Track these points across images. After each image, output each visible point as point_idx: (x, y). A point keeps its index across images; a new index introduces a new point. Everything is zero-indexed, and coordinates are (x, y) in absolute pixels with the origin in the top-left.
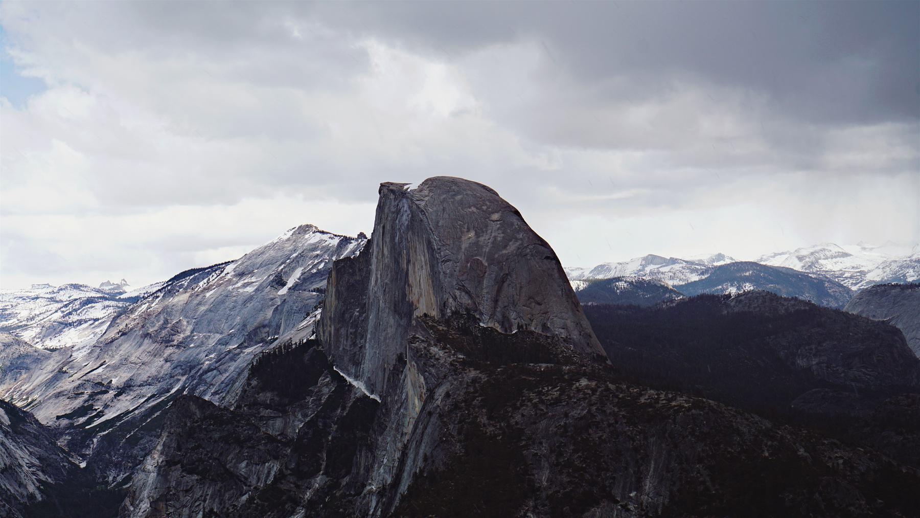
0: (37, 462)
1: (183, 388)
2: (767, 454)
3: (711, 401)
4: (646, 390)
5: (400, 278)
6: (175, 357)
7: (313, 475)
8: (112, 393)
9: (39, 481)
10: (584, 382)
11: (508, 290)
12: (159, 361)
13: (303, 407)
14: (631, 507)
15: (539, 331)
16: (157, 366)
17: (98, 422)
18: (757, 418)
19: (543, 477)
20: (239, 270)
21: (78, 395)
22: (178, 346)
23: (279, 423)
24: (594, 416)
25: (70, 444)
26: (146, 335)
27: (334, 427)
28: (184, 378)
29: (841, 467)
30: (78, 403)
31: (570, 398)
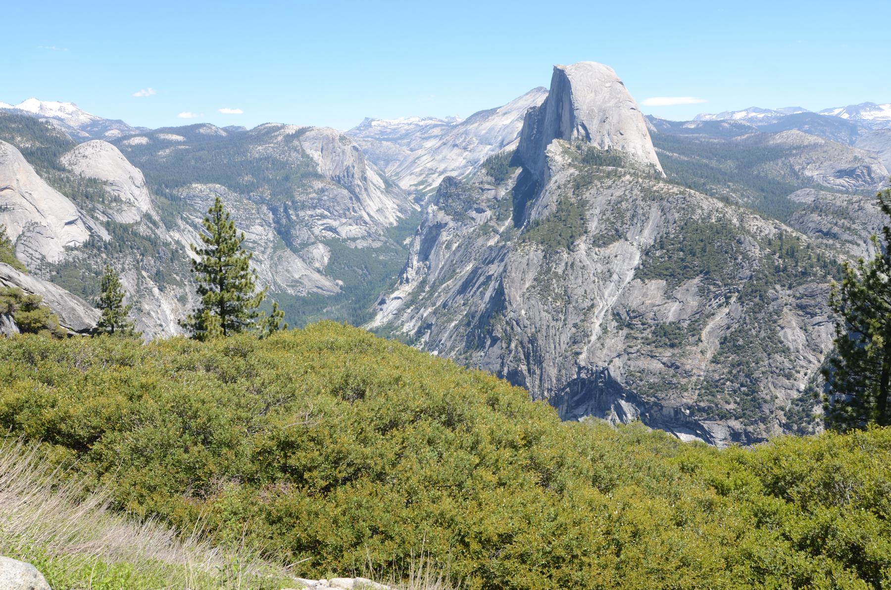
0: (396, 207)
1: (470, 173)
2: (714, 221)
3: (692, 191)
4: (658, 183)
5: (559, 117)
6: (468, 157)
7: (507, 219)
8: (437, 175)
9: (397, 216)
10: (628, 177)
11: (607, 126)
12: (461, 159)
13: (507, 185)
14: (635, 244)
15: (620, 149)
16: (461, 162)
17: (429, 188)
18: (715, 201)
19: (593, 226)
20: (504, 111)
21: (421, 175)
22: (470, 151)
23: (493, 192)
24: (626, 196)
25: (415, 199)
26: (455, 145)
27: (520, 196)
28: (471, 168)
29: (755, 230)
30: (421, 178)
31: (617, 185)
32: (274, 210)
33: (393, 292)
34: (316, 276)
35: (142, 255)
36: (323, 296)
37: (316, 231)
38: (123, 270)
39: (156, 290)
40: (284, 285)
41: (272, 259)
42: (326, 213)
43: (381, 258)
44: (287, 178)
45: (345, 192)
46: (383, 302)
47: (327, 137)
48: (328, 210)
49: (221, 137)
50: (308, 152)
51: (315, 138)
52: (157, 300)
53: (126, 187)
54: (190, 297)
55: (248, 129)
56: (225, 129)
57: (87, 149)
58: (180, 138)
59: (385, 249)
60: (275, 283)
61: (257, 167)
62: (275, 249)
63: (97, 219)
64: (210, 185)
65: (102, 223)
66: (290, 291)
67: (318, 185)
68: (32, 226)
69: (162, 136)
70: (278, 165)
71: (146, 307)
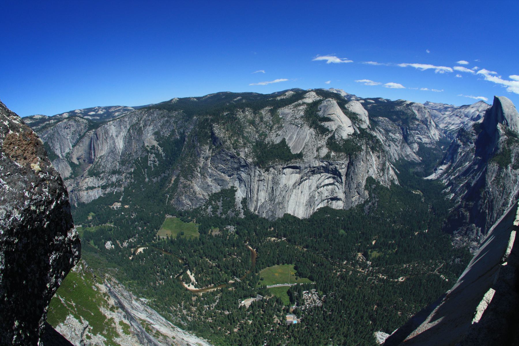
32: (403, 129)
33: (439, 167)
34: (414, 154)
35: (368, 140)
36: (415, 162)
37: (415, 139)
38: (363, 144)
39: (371, 152)
40: (404, 156)
41: (401, 146)
42: (419, 133)
43: (434, 152)
44: (407, 118)
45: (425, 126)
46: (436, 170)
47: (420, 107)
48: (419, 131)
49: (385, 102)
50: (414, 110)
51: (416, 106)
52: (371, 156)
53: (363, 116)
54: (381, 157)
55: (392, 100)
56: (387, 100)
57: (351, 103)
58: (373, 102)
59: (435, 149)
60: (401, 155)
61: (397, 113)
62: (402, 143)
63: (356, 126)
64: (384, 118)
65: (357, 127)
66: (406, 159)
67: (417, 123)
68: (339, 127)
69: (368, 101)
70: (404, 114)
71: (368, 158)
